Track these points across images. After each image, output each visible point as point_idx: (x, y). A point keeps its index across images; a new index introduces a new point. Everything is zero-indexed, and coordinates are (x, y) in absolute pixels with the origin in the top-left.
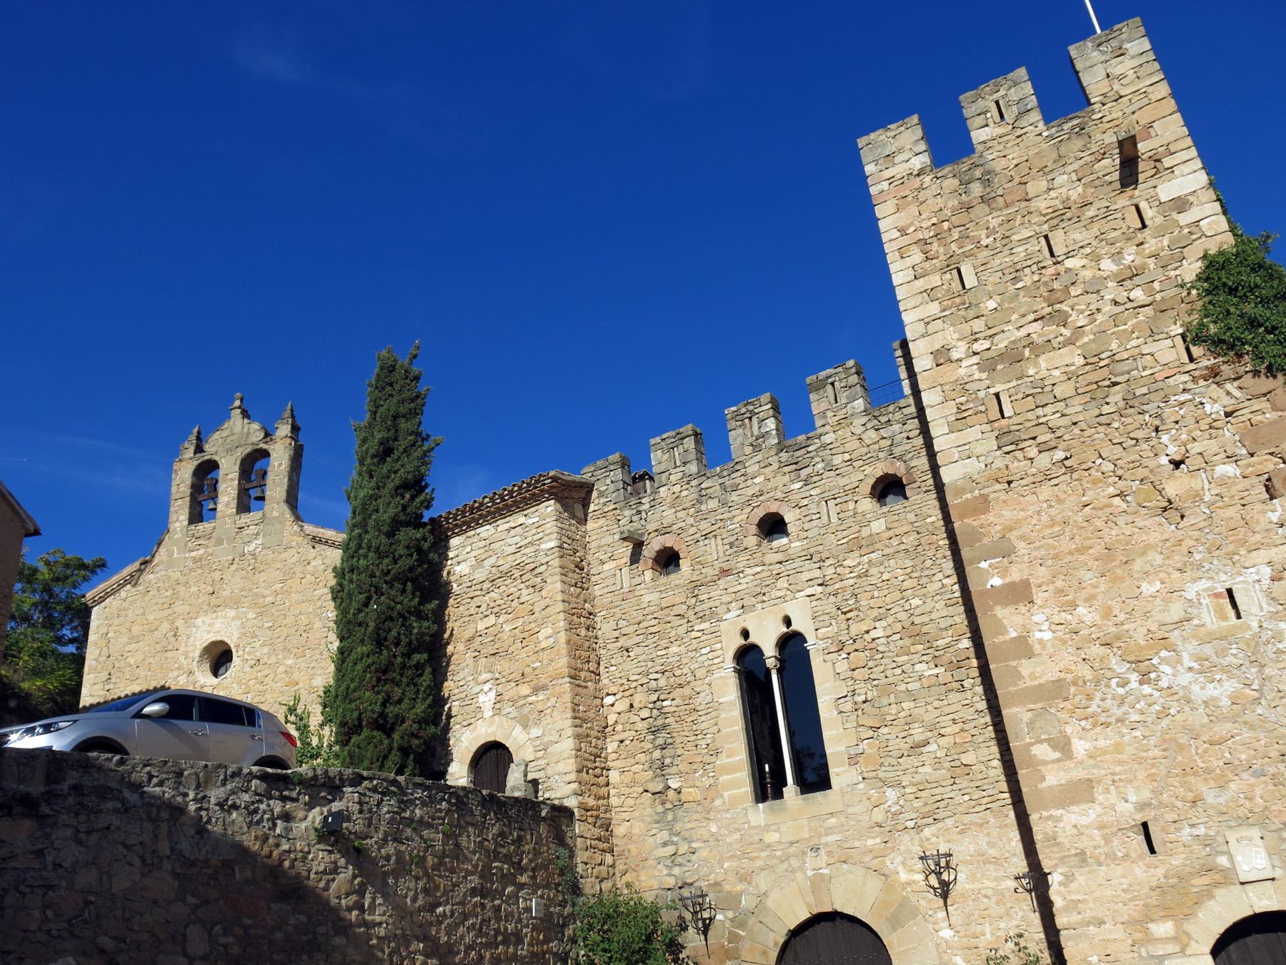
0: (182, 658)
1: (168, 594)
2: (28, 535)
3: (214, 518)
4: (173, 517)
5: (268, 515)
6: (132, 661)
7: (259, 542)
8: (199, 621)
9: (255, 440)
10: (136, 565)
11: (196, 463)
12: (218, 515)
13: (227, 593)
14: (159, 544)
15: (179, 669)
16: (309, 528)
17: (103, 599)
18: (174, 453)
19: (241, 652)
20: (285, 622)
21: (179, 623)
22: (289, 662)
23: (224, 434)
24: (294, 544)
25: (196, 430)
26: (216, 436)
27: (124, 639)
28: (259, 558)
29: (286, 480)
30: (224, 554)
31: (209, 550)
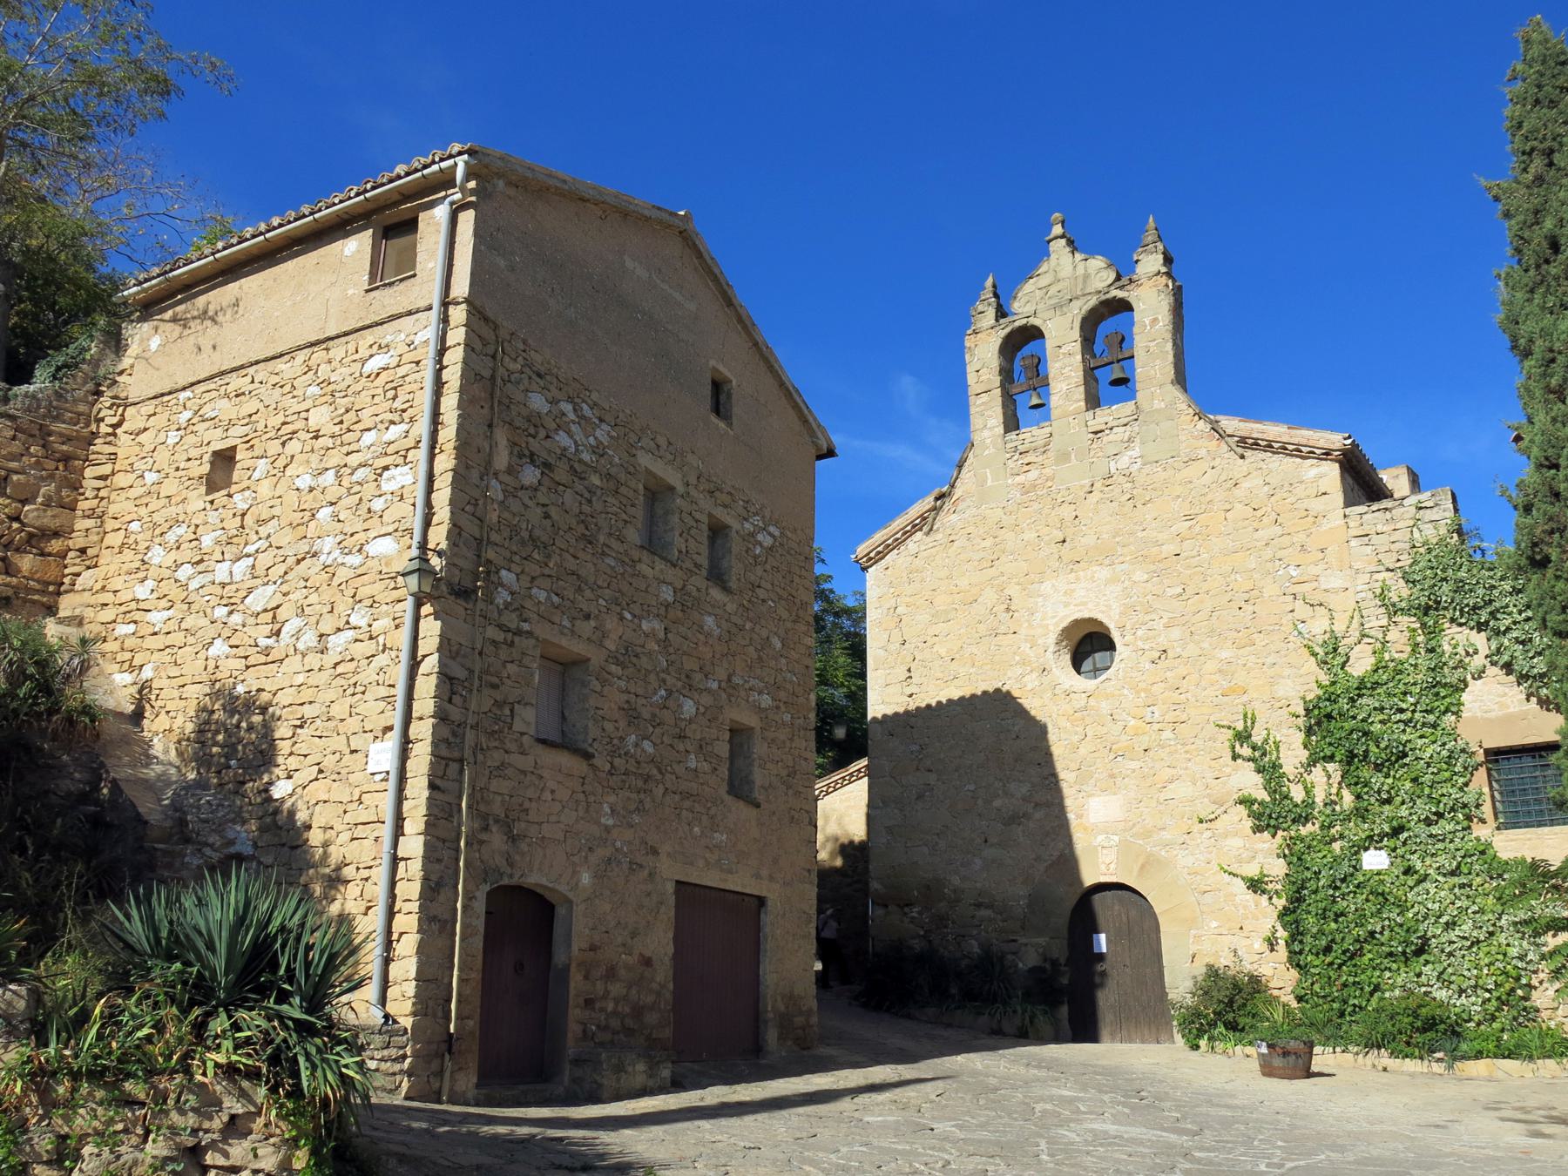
0: (1025, 647)
1: (988, 543)
2: (820, 457)
3: (1047, 418)
4: (976, 421)
5: (1144, 405)
6: (943, 652)
8: (1046, 587)
9: (1101, 285)
10: (928, 502)
11: (1003, 333)
12: (1054, 413)
13: (1090, 540)
14: (960, 467)
15: (1023, 663)
16: (1230, 424)
17: (881, 556)
18: (963, 323)
19: (1129, 638)
20: (1205, 587)
21: (1013, 590)
22: (1225, 654)
23: (1043, 281)
24: (1202, 453)
25: (989, 282)
26: (1029, 286)
29: (1169, 346)
31: (1047, 471)
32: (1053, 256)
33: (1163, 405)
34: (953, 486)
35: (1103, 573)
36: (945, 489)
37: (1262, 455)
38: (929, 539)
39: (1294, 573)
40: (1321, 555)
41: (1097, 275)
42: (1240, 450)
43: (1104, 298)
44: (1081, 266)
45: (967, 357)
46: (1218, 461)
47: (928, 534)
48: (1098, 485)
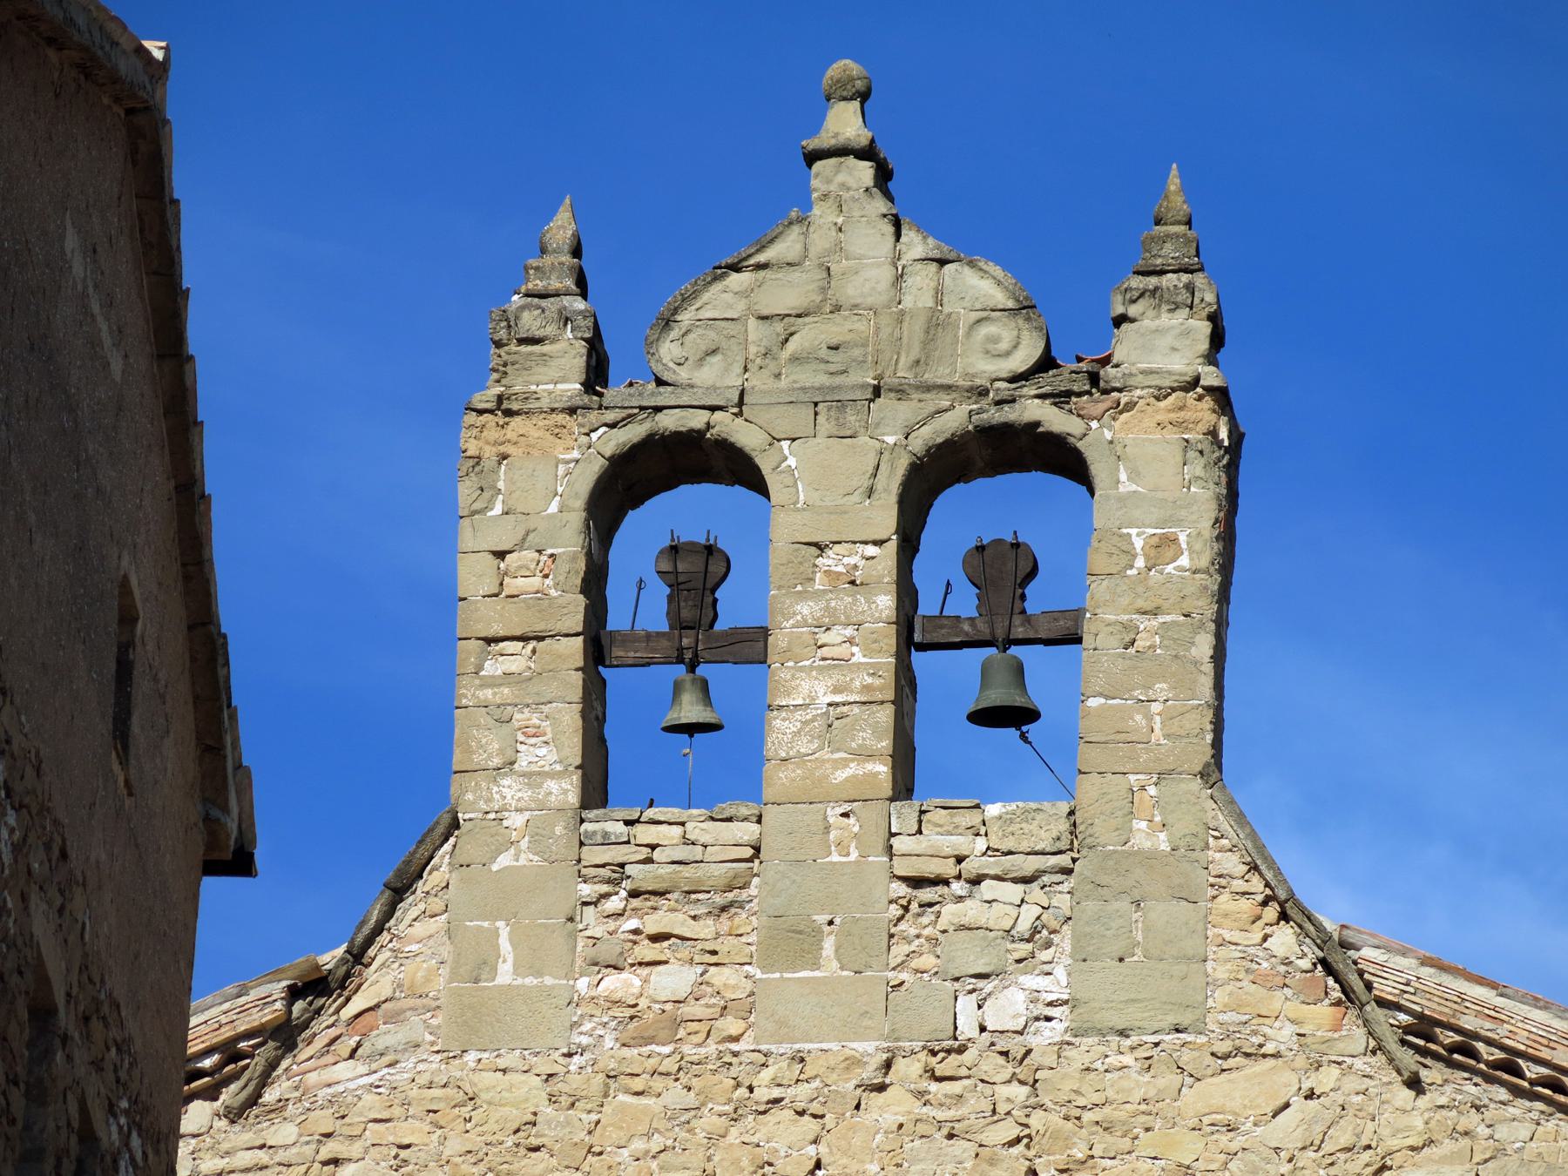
2: (214, 868)
4: (478, 742)
5: (1101, 830)
7: (1055, 985)
9: (989, 369)
11: (613, 441)
24: (1281, 1036)
28: (1062, 1082)
30: (823, 1014)
32: (822, 214)
33: (1163, 842)
34: (357, 957)
36: (330, 958)
37: (1472, 1090)
38: (241, 1135)
41: (977, 329)
42: (1408, 1058)
43: (996, 416)
44: (921, 283)
45: (466, 491)
46: (1327, 1078)
47: (235, 1115)
48: (909, 1069)
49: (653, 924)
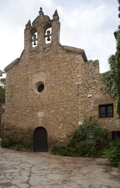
8: (34, 76)
9: (47, 21)
27: (15, 81)
35: (43, 74)
39: (73, 74)
40: (77, 71)
47: (16, 66)
49: (33, 53)
